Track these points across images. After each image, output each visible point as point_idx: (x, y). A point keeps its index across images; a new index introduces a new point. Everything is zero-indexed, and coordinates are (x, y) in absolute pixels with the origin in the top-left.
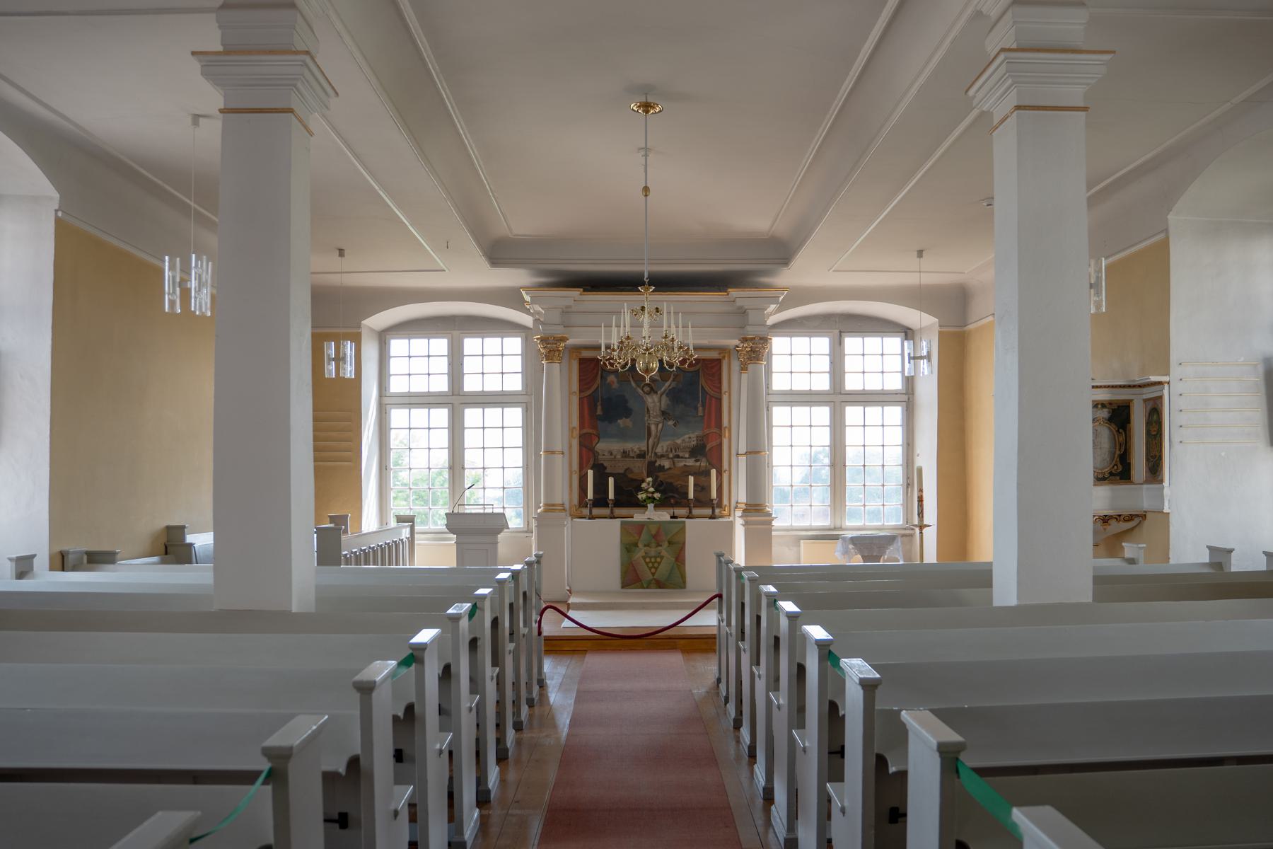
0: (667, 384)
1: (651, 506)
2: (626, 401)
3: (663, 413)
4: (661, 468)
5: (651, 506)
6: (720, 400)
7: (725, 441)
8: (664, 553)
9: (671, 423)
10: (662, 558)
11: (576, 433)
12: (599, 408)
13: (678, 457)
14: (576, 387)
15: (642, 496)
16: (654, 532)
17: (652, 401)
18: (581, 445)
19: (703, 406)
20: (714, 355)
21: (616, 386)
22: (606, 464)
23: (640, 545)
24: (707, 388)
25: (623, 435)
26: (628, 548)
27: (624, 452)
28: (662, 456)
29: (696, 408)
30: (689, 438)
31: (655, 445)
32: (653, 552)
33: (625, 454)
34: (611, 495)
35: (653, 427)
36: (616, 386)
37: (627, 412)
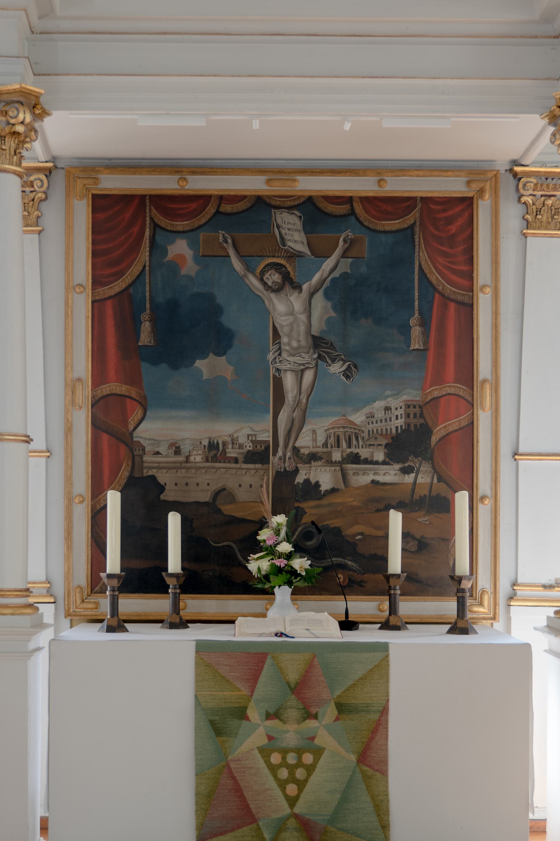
0: (328, 264)
1: (283, 593)
2: (218, 310)
3: (317, 342)
4: (311, 490)
5: (283, 593)
6: (468, 309)
7: (483, 421)
8: (324, 739)
9: (337, 368)
10: (318, 752)
11: (85, 394)
12: (146, 327)
13: (355, 459)
14: (83, 270)
15: (258, 565)
16: (293, 676)
17: (286, 309)
18: (97, 426)
19: (424, 323)
20: (455, 187)
21: (190, 268)
22: (163, 478)
23: (254, 713)
24: (434, 277)
25: (210, 400)
26: (218, 723)
27: (212, 446)
28: (313, 457)
29: (405, 330)
30: (385, 407)
31: (296, 428)
32: (290, 734)
33: (215, 451)
34: (174, 563)
35: (289, 381)
36: (190, 268)
37: (221, 340)
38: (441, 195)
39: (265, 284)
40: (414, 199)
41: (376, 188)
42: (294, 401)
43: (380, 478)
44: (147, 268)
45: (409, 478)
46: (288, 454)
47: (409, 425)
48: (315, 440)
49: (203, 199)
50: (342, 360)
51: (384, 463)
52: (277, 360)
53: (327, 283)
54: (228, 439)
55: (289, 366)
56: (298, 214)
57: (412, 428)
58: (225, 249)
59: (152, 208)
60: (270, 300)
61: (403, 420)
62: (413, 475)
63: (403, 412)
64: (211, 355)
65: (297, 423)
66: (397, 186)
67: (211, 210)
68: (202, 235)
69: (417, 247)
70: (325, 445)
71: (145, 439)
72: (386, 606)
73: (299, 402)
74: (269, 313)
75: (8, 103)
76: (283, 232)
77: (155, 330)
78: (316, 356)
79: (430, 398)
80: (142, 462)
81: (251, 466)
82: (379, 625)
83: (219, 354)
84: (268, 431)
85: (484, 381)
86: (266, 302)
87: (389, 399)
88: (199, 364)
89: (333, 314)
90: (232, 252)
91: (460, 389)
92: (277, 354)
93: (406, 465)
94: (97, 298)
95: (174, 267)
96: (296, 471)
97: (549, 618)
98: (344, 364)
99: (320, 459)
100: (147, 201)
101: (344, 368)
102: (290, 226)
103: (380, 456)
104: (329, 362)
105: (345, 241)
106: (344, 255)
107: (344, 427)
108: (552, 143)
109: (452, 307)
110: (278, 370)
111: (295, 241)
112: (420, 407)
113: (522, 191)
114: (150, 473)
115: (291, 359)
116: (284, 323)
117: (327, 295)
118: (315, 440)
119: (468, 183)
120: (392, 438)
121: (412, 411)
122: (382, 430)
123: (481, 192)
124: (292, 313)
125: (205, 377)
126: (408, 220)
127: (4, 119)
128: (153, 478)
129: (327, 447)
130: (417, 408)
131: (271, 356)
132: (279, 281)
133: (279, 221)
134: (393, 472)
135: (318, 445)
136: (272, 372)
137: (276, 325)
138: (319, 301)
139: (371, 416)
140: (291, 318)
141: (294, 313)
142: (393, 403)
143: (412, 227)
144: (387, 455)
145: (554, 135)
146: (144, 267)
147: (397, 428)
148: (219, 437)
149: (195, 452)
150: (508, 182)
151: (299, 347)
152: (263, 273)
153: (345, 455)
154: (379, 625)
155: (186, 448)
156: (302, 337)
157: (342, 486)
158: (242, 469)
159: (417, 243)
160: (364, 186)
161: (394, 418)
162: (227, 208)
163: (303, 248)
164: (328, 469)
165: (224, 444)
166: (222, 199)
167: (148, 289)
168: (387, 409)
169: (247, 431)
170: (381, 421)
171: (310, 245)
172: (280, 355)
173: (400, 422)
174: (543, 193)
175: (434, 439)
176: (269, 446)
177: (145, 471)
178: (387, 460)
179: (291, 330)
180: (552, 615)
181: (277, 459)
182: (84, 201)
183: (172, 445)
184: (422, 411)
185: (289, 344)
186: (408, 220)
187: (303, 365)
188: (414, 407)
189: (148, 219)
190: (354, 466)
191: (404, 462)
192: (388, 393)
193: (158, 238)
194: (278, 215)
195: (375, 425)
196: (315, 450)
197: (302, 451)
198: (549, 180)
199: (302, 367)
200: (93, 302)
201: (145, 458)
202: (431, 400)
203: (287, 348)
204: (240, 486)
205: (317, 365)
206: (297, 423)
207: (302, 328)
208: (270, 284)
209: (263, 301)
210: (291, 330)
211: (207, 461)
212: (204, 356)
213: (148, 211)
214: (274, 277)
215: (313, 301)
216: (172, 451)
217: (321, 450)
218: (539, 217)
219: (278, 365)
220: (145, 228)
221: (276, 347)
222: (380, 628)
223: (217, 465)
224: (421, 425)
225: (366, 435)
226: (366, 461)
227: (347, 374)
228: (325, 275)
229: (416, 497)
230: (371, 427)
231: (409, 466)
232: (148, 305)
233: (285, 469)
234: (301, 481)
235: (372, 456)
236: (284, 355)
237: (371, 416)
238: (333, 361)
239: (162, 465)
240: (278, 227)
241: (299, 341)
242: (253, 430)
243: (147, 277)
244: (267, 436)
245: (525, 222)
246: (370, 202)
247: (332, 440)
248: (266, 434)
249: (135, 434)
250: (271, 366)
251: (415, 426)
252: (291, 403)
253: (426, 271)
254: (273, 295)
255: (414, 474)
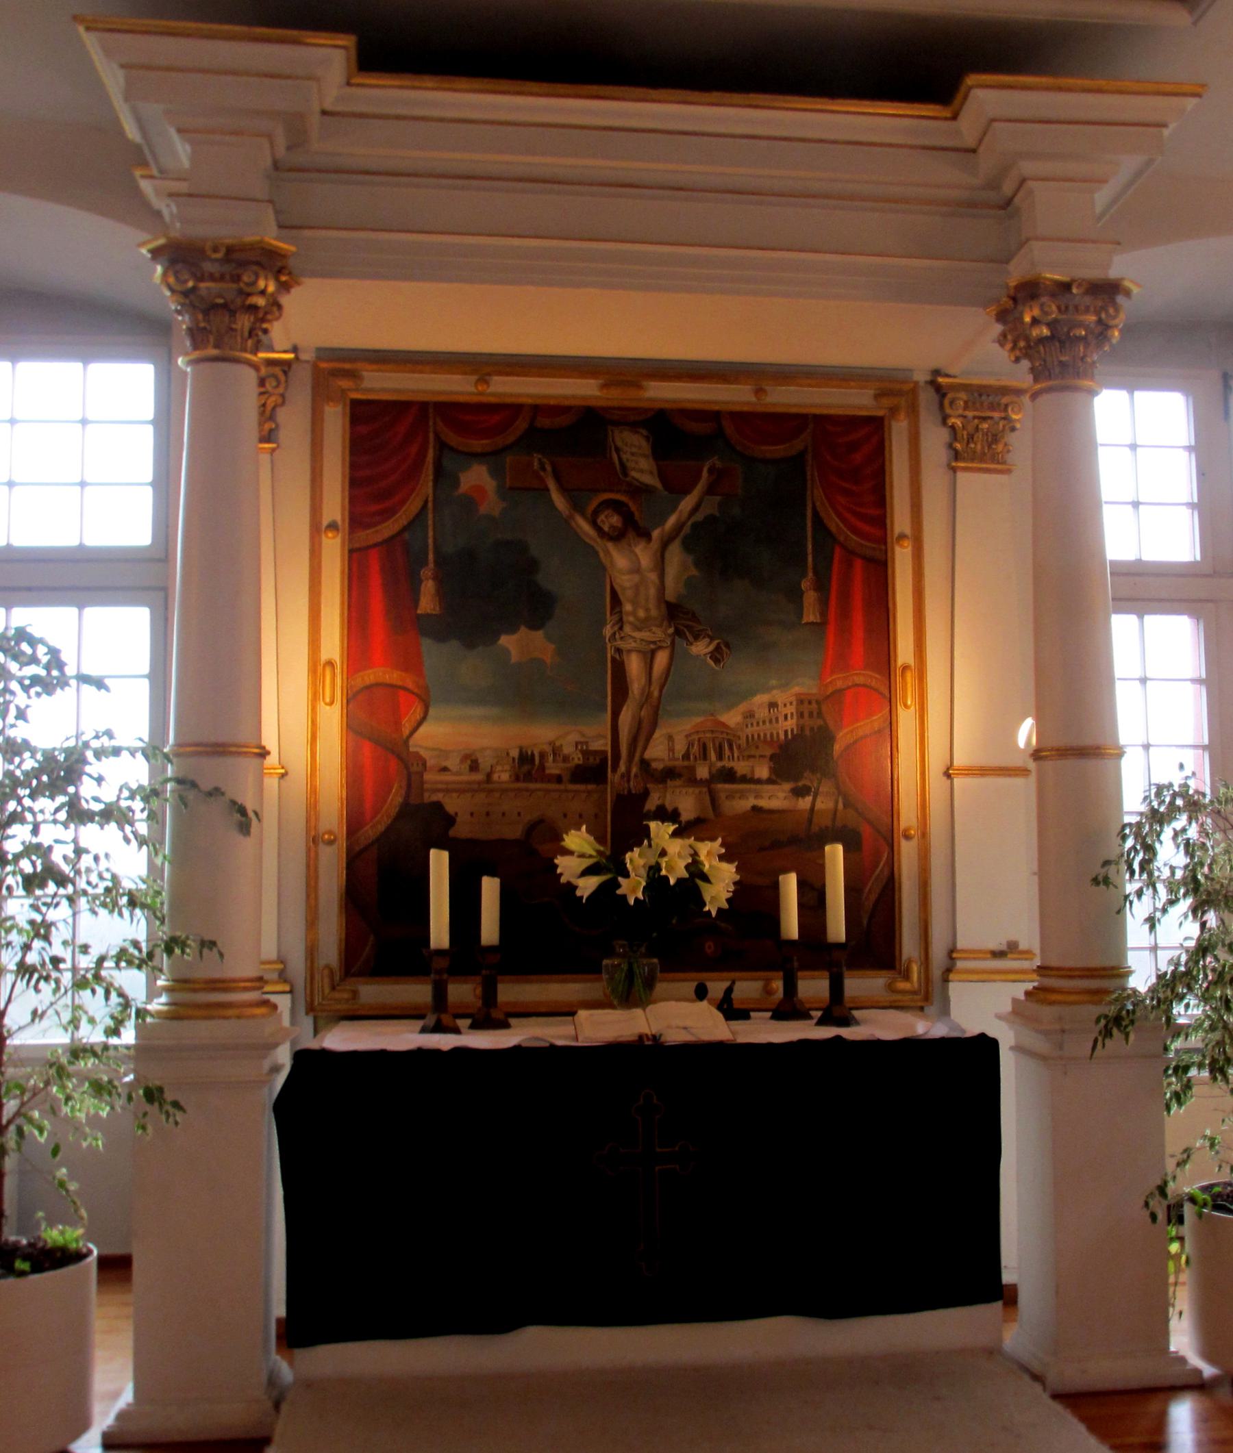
0: (687, 503)
2: (533, 566)
3: (674, 612)
9: (701, 648)
12: (428, 587)
13: (729, 776)
17: (628, 565)
19: (821, 586)
20: (859, 401)
22: (452, 805)
24: (834, 523)
27: (525, 758)
28: (670, 774)
29: (795, 596)
31: (643, 732)
35: (634, 665)
36: (492, 505)
37: (536, 607)
38: (841, 412)
39: (599, 529)
40: (804, 417)
41: (754, 399)
42: (642, 694)
43: (763, 803)
44: (430, 505)
45: (805, 803)
46: (634, 770)
47: (802, 728)
48: (671, 750)
49: (510, 410)
50: (709, 636)
51: (770, 781)
52: (617, 636)
53: (687, 529)
54: (548, 749)
55: (633, 645)
56: (645, 432)
57: (807, 732)
58: (542, 480)
59: (438, 419)
60: (607, 553)
61: (794, 721)
62: (809, 799)
63: (794, 711)
64: (523, 629)
65: (646, 725)
66: (783, 398)
67: (521, 425)
68: (509, 459)
69: (809, 482)
70: (686, 756)
71: (427, 748)
72: (778, 985)
73: (649, 695)
74: (604, 569)
75: (243, 264)
76: (624, 457)
77: (441, 593)
78: (671, 630)
79: (830, 690)
80: (422, 783)
81: (582, 787)
82: (769, 1014)
83: (534, 627)
84: (605, 737)
85: (905, 668)
86: (602, 555)
87: (775, 692)
88: (505, 640)
89: (694, 572)
90: (552, 485)
91: (873, 678)
92: (616, 628)
93: (800, 784)
94: (357, 545)
95: (469, 503)
96: (646, 794)
97: (1015, 1001)
98: (710, 643)
99: (680, 776)
100: (431, 410)
101: (711, 648)
102: (634, 450)
103: (763, 772)
104: (691, 638)
105: (710, 471)
106: (710, 490)
107: (712, 732)
108: (1002, 345)
109: (858, 565)
110: (619, 650)
111: (642, 471)
112: (818, 702)
113: (948, 411)
114: (435, 798)
115: (637, 634)
116: (627, 584)
117: (687, 546)
118: (671, 750)
119: (877, 397)
120: (781, 747)
121: (806, 709)
122: (765, 735)
123: (894, 411)
124: (637, 570)
125: (513, 660)
126: (798, 445)
127: (234, 286)
128: (438, 806)
129: (689, 759)
130: (814, 706)
131: (608, 631)
132: (620, 525)
133: (619, 444)
134: (782, 795)
135: (676, 755)
136: (610, 653)
137: (616, 587)
138: (675, 555)
139: (750, 715)
140: (636, 578)
141: (637, 569)
142: (779, 696)
143: (802, 455)
144: (772, 770)
145: (1004, 335)
146: (426, 502)
147: (786, 732)
148: (535, 745)
149: (499, 768)
150: (926, 398)
151: (647, 619)
152: (596, 513)
153: (714, 771)
154: (769, 1014)
155: (485, 762)
156: (652, 605)
157: (710, 814)
158: (567, 791)
159: (809, 477)
160: (736, 396)
161: (781, 719)
162: (544, 422)
163: (651, 480)
164: (691, 790)
165: (543, 755)
166: (538, 409)
167: (431, 534)
168: (773, 705)
169: (574, 737)
170: (764, 722)
171: (662, 476)
172: (621, 628)
173: (791, 724)
174: (976, 414)
175: (837, 748)
176: (606, 759)
177: (426, 795)
178: (774, 777)
179: (637, 594)
180: (1022, 997)
181: (617, 778)
182: (339, 409)
183: (466, 757)
184: (820, 709)
185: (634, 613)
186: (798, 445)
187: (654, 643)
188: (810, 703)
189: (431, 435)
190: (727, 786)
191: (796, 779)
192: (774, 682)
193: (446, 462)
194: (616, 432)
195: (755, 728)
196: (671, 764)
197: (654, 765)
198: (984, 398)
199: (652, 646)
200: (351, 551)
201: (427, 777)
202: (833, 693)
203: (631, 619)
204: (565, 816)
205: (673, 643)
206: (646, 725)
207: (652, 591)
208: (606, 529)
209: (597, 553)
210: (637, 594)
211: (517, 779)
212: (512, 630)
213: (431, 423)
214: (611, 520)
215: (667, 555)
216: (466, 766)
217: (679, 763)
218: (972, 446)
219: (619, 643)
220: (426, 451)
221: (616, 617)
222: (772, 1018)
223: (532, 786)
224: (820, 728)
225: (743, 742)
226: (744, 779)
227: (716, 656)
228: (683, 519)
229: (815, 828)
230: (749, 730)
231: (804, 786)
232: (431, 556)
233: (630, 791)
234: (653, 808)
235: (753, 772)
236: (627, 629)
237: (750, 715)
238: (696, 638)
239: (450, 786)
240: (618, 450)
241: (647, 610)
242: (583, 735)
243: (430, 516)
244: (602, 744)
245: (953, 453)
246: (744, 419)
247: (695, 749)
248: (602, 742)
249: (411, 742)
250: (609, 646)
251: (812, 729)
252: (637, 697)
253: (822, 514)
254: (610, 545)
255: (811, 798)
